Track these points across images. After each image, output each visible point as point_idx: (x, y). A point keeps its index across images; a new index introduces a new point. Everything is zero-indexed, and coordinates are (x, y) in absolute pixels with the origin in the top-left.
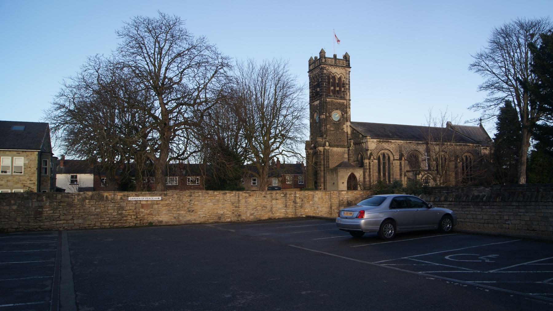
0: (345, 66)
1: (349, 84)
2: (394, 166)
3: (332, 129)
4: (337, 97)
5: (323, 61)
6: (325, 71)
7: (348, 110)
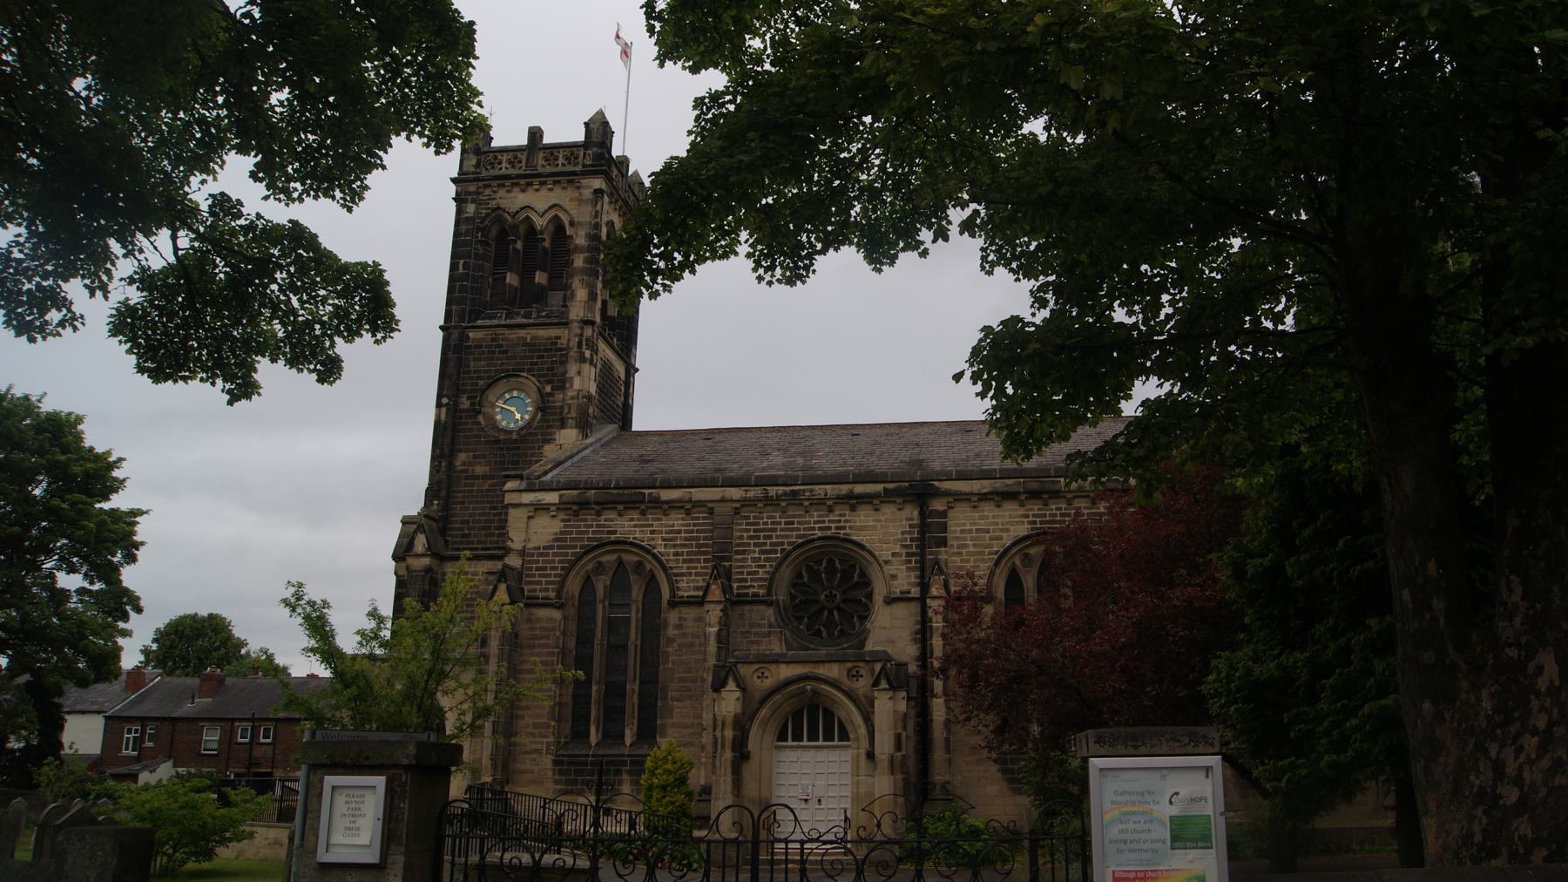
0: (578, 169)
2: (670, 641)
3: (480, 470)
4: (525, 317)
5: (465, 169)
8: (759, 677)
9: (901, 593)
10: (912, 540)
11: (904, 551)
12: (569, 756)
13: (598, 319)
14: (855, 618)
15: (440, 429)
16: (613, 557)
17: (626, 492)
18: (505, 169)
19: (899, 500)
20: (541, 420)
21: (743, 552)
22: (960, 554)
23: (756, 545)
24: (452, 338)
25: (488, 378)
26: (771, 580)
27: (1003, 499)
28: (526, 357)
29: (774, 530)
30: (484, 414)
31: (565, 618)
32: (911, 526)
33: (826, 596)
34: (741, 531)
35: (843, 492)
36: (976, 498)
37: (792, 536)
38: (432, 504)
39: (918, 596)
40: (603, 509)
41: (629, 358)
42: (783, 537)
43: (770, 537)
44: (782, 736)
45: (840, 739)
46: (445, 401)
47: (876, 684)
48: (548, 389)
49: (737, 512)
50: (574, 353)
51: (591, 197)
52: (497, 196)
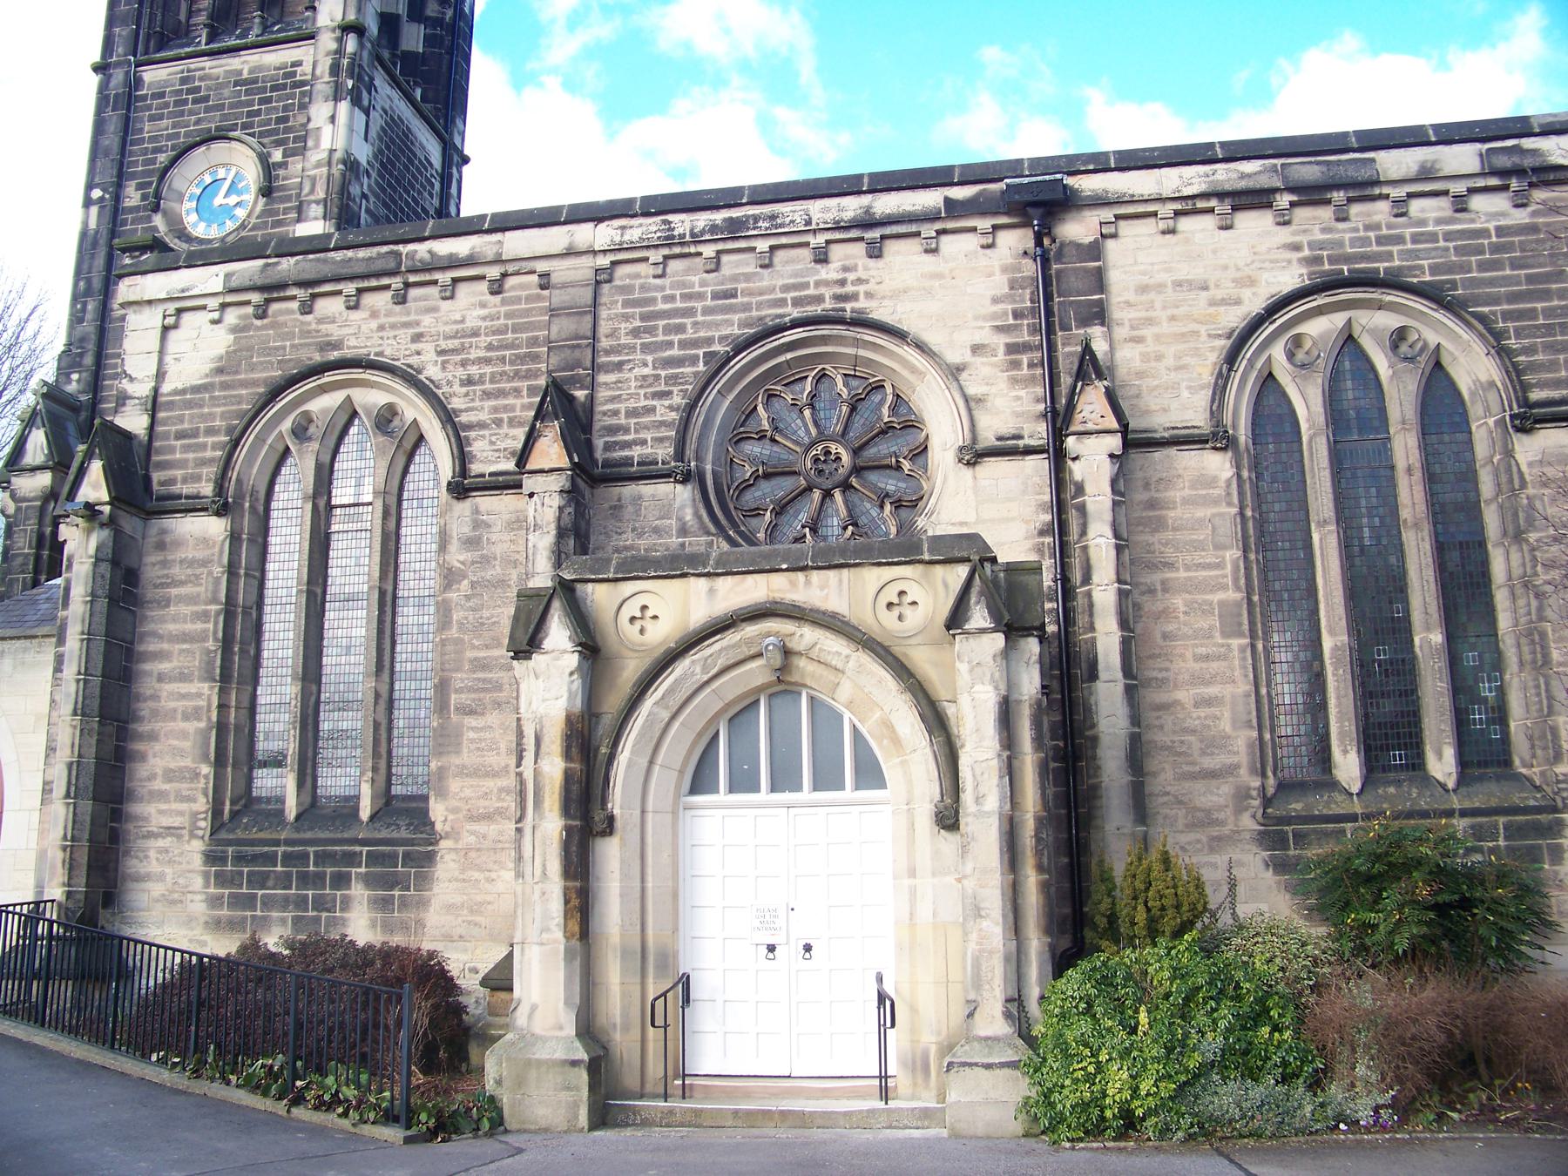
8: (633, 619)
9: (1000, 439)
10: (1017, 315)
11: (1001, 341)
12: (239, 842)
13: (373, 28)
14: (888, 508)
15: (87, 242)
16: (332, 400)
17: (362, 253)
19: (984, 224)
20: (264, 213)
21: (619, 366)
22: (1138, 340)
23: (646, 348)
24: (112, 85)
25: (173, 149)
26: (684, 427)
27: (1235, 209)
28: (241, 104)
29: (689, 312)
30: (165, 214)
31: (235, 537)
32: (1013, 285)
33: (816, 460)
34: (615, 321)
35: (848, 215)
36: (1167, 209)
37: (729, 323)
38: (69, 381)
39: (1041, 442)
40: (314, 296)
41: (451, 134)
42: (717, 325)
43: (680, 329)
44: (701, 781)
45: (858, 786)
46: (97, 193)
47: (956, 620)
48: (277, 156)
49: (602, 278)
50: (323, 86)
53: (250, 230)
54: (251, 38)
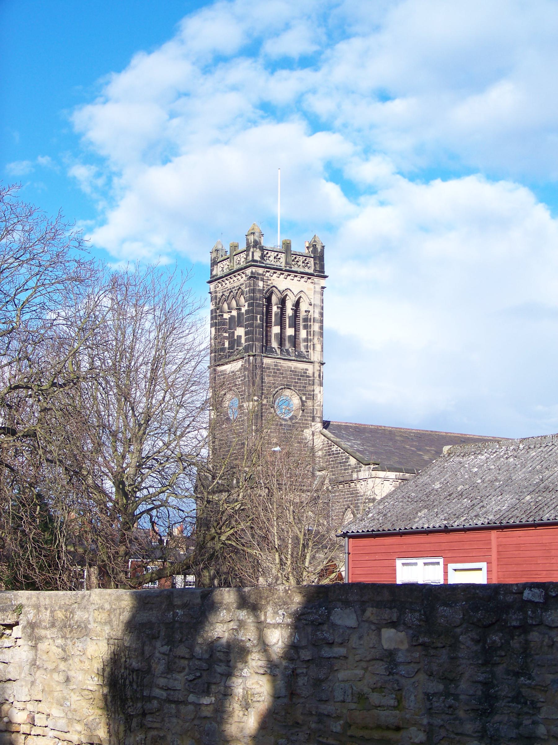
1: (322, 322)
6: (261, 284)
7: (317, 389)
18: (271, 260)
51: (320, 290)
52: (272, 278)
53: (299, 420)
54: (293, 358)
